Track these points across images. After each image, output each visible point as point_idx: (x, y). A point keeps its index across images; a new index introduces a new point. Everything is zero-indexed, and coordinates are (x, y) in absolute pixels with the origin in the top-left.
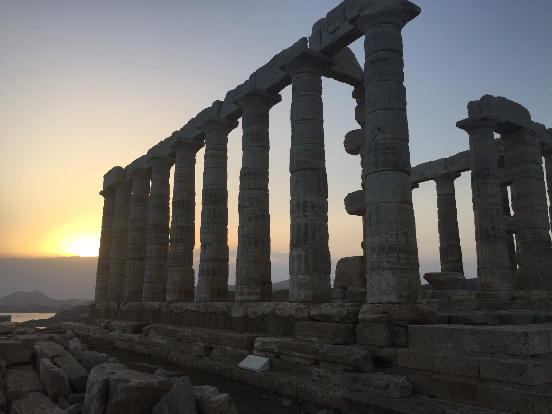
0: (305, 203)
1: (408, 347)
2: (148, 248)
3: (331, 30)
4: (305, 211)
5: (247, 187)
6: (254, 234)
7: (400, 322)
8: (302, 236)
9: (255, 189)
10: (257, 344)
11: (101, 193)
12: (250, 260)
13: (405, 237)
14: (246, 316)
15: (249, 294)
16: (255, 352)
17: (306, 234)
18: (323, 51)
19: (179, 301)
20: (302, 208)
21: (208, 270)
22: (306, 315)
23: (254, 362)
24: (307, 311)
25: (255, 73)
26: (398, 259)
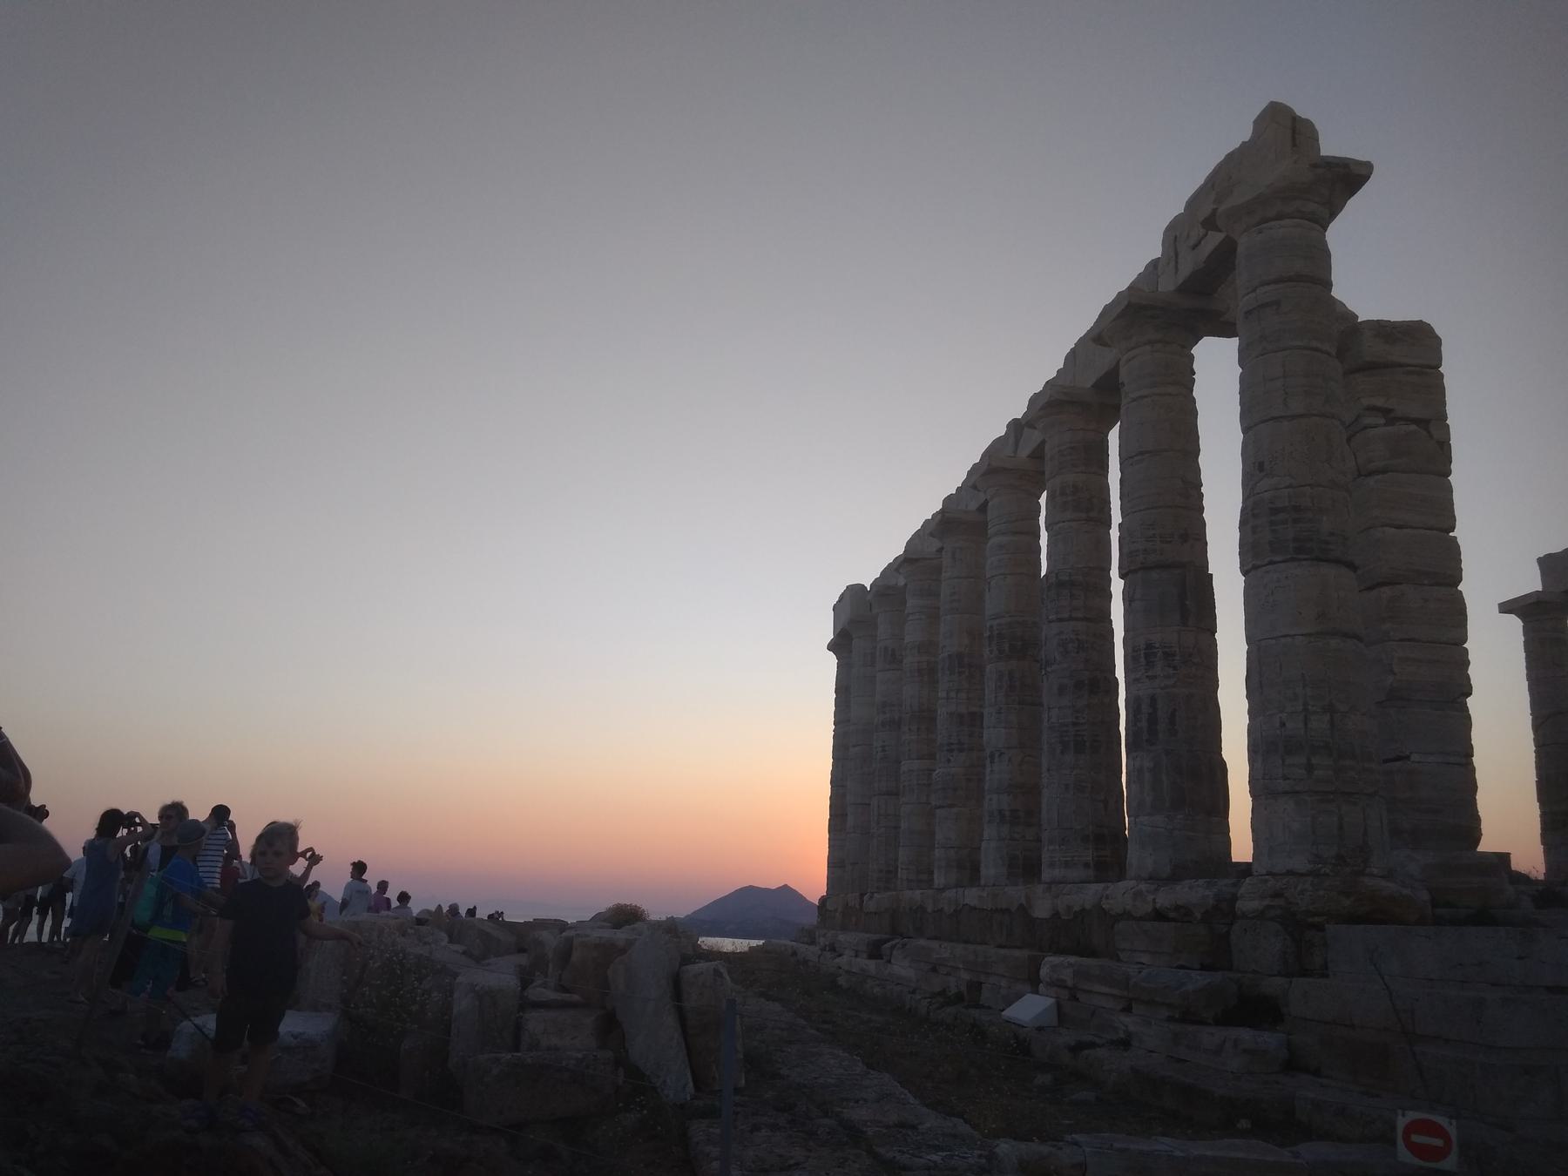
0: (1149, 646)
1: (1327, 976)
3: (1192, 242)
4: (1150, 664)
6: (1075, 724)
7: (1317, 919)
8: (1144, 724)
9: (1071, 619)
10: (1044, 972)
11: (830, 647)
14: (1056, 914)
15: (1067, 865)
18: (1182, 289)
21: (1000, 811)
22: (1149, 908)
23: (1029, 1009)
24: (1150, 898)
25: (1073, 351)
26: (1310, 768)
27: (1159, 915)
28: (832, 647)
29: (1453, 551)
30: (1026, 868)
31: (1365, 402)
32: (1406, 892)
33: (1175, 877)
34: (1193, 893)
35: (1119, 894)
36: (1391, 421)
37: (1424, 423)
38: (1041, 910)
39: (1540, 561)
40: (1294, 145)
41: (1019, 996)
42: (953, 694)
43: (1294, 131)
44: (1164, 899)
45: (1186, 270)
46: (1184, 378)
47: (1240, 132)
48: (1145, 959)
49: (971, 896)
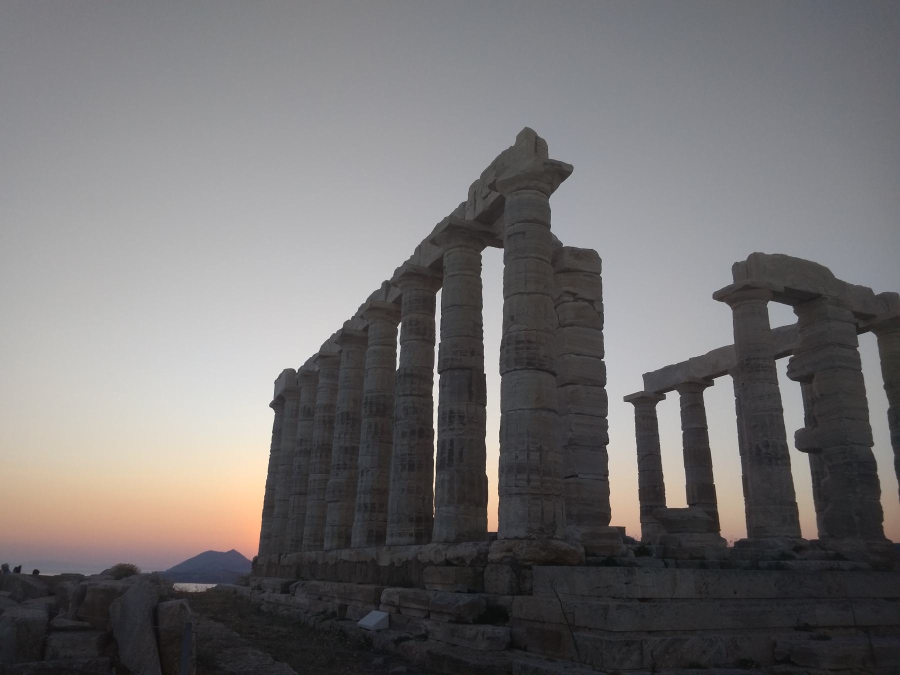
0: (451, 412)
2: (312, 477)
3: (484, 195)
4: (451, 422)
5: (400, 393)
6: (409, 454)
7: (528, 563)
8: (446, 455)
9: (411, 395)
10: (383, 597)
11: (271, 406)
12: (403, 490)
13: (538, 454)
14: (393, 564)
15: (400, 535)
16: (381, 606)
17: (451, 452)
18: (478, 219)
19: (339, 548)
20: (448, 420)
21: (365, 505)
23: (374, 619)
25: (420, 246)
26: (529, 481)
27: (448, 563)
28: (272, 405)
29: (602, 368)
30: (377, 537)
31: (565, 288)
32: (573, 548)
33: (457, 541)
34: (466, 550)
35: (428, 552)
36: (576, 300)
37: (591, 302)
38: (384, 562)
39: (644, 376)
40: (536, 151)
41: (368, 612)
42: (342, 436)
43: (536, 143)
44: (451, 553)
45: (480, 208)
46: (476, 267)
47: (510, 142)
48: (439, 588)
49: (345, 554)
